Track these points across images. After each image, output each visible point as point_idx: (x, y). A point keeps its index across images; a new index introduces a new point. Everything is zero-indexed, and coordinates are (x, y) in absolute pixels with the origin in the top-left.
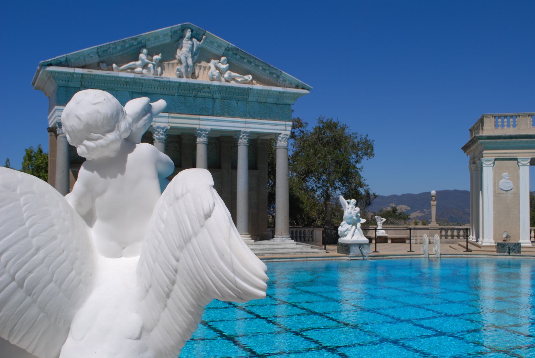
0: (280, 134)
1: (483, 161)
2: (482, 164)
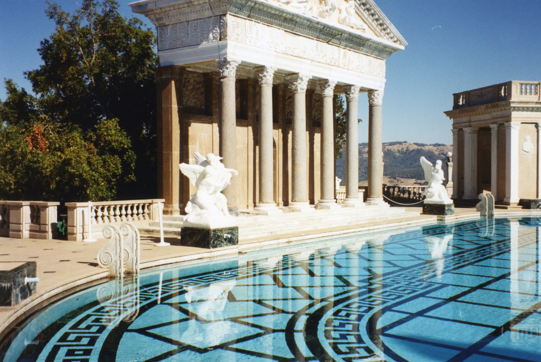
0: (376, 90)
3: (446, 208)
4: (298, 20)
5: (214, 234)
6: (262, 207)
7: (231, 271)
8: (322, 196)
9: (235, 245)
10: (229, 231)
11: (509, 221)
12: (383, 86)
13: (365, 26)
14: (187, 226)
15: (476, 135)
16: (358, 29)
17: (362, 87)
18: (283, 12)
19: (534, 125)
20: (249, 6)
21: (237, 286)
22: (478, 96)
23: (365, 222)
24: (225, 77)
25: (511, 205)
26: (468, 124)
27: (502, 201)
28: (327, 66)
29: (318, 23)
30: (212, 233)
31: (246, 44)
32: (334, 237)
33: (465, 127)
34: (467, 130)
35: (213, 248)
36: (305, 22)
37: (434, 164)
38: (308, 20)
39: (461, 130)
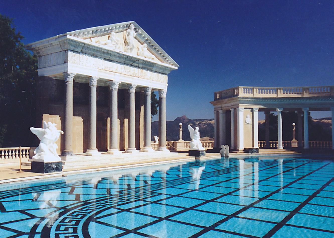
0: (163, 90)
1: (240, 109)
2: (239, 110)
3: (200, 153)
4: (111, 53)
5: (46, 166)
6: (89, 152)
7: (59, 185)
8: (129, 146)
9: (60, 171)
10: (56, 164)
11: (238, 160)
12: (167, 88)
13: (154, 57)
14: (34, 161)
15: (225, 114)
16: (149, 58)
17: (153, 88)
18: (101, 49)
19: (250, 110)
20: (81, 45)
21: (62, 193)
22: (225, 94)
23: (151, 160)
24: (67, 82)
25: (240, 151)
26: (220, 108)
27: (234, 149)
28: (131, 77)
29: (124, 55)
30: (45, 165)
31: (80, 65)
32: (128, 168)
33: (220, 110)
34: (220, 112)
35: (45, 173)
36: (116, 54)
37: (195, 129)
38: (118, 53)
39: (218, 111)
